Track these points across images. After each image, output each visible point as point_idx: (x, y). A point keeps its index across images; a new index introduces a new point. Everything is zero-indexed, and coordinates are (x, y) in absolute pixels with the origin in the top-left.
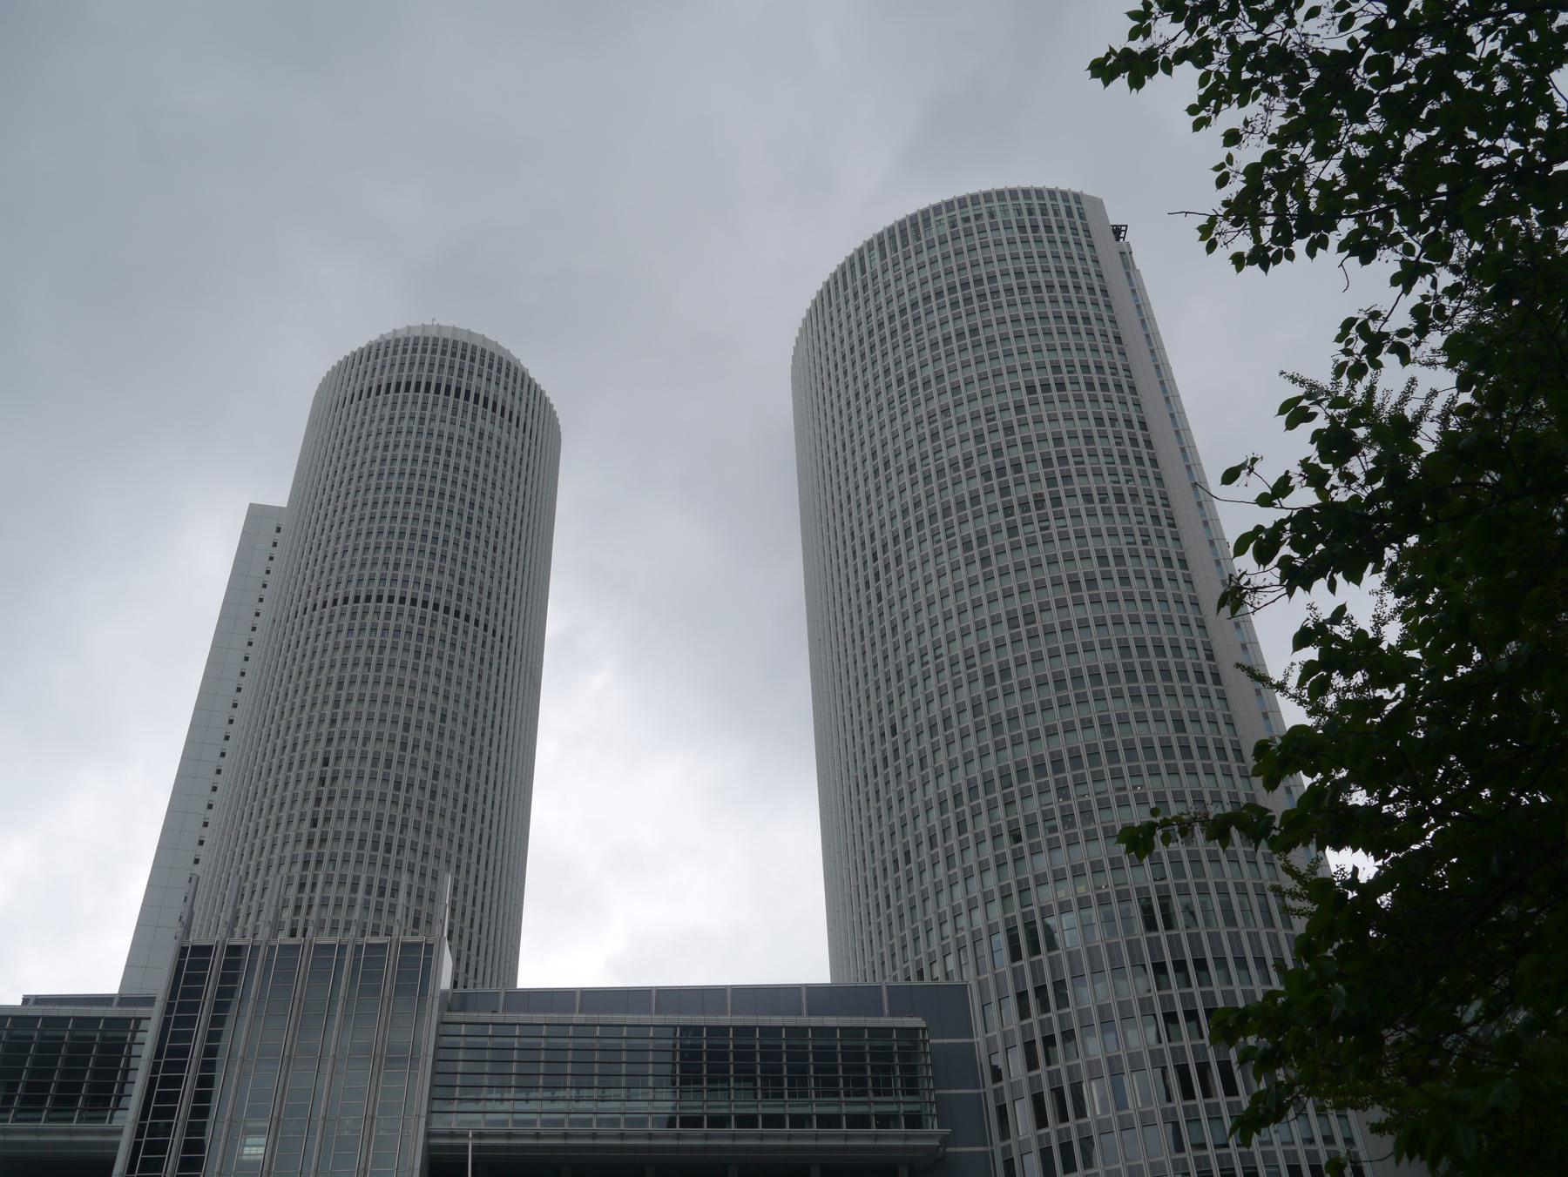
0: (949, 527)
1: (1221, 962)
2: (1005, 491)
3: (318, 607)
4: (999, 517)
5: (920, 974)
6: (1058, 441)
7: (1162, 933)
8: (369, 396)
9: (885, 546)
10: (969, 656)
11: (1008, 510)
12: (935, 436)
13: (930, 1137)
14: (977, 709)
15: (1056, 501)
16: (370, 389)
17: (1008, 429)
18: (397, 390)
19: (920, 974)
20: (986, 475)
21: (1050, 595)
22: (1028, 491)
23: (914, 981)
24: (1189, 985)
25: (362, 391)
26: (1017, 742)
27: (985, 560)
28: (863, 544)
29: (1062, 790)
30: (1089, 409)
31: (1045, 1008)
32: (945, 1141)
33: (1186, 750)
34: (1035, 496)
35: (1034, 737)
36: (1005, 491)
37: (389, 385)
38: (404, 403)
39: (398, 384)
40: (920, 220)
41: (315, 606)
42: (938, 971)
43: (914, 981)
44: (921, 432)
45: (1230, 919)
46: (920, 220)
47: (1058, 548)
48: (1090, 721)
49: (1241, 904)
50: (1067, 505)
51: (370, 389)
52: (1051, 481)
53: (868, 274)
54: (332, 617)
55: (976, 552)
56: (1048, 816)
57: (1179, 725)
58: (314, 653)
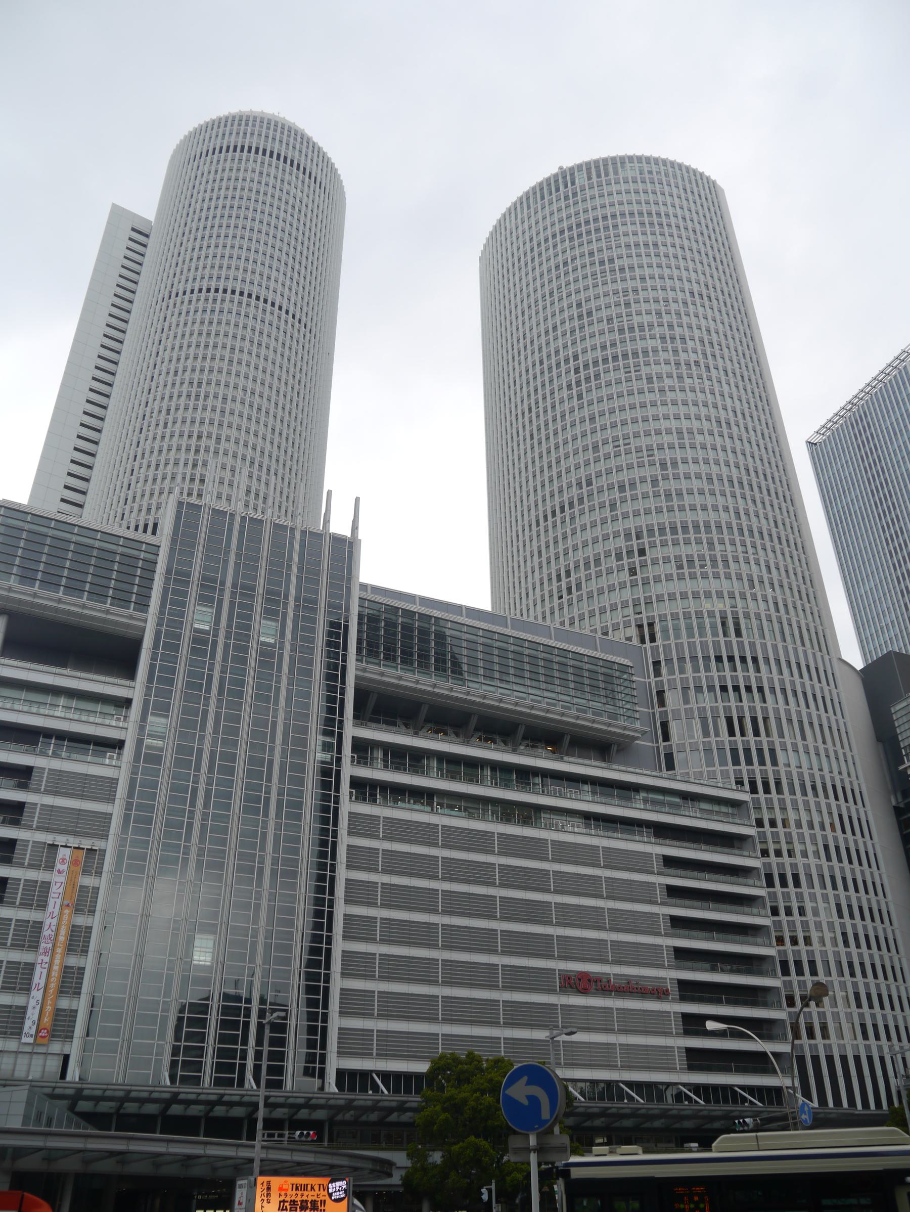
2: (675, 351)
11: (678, 364)
12: (628, 305)
13: (636, 731)
14: (655, 482)
29: (711, 544)
52: (705, 355)
56: (702, 558)
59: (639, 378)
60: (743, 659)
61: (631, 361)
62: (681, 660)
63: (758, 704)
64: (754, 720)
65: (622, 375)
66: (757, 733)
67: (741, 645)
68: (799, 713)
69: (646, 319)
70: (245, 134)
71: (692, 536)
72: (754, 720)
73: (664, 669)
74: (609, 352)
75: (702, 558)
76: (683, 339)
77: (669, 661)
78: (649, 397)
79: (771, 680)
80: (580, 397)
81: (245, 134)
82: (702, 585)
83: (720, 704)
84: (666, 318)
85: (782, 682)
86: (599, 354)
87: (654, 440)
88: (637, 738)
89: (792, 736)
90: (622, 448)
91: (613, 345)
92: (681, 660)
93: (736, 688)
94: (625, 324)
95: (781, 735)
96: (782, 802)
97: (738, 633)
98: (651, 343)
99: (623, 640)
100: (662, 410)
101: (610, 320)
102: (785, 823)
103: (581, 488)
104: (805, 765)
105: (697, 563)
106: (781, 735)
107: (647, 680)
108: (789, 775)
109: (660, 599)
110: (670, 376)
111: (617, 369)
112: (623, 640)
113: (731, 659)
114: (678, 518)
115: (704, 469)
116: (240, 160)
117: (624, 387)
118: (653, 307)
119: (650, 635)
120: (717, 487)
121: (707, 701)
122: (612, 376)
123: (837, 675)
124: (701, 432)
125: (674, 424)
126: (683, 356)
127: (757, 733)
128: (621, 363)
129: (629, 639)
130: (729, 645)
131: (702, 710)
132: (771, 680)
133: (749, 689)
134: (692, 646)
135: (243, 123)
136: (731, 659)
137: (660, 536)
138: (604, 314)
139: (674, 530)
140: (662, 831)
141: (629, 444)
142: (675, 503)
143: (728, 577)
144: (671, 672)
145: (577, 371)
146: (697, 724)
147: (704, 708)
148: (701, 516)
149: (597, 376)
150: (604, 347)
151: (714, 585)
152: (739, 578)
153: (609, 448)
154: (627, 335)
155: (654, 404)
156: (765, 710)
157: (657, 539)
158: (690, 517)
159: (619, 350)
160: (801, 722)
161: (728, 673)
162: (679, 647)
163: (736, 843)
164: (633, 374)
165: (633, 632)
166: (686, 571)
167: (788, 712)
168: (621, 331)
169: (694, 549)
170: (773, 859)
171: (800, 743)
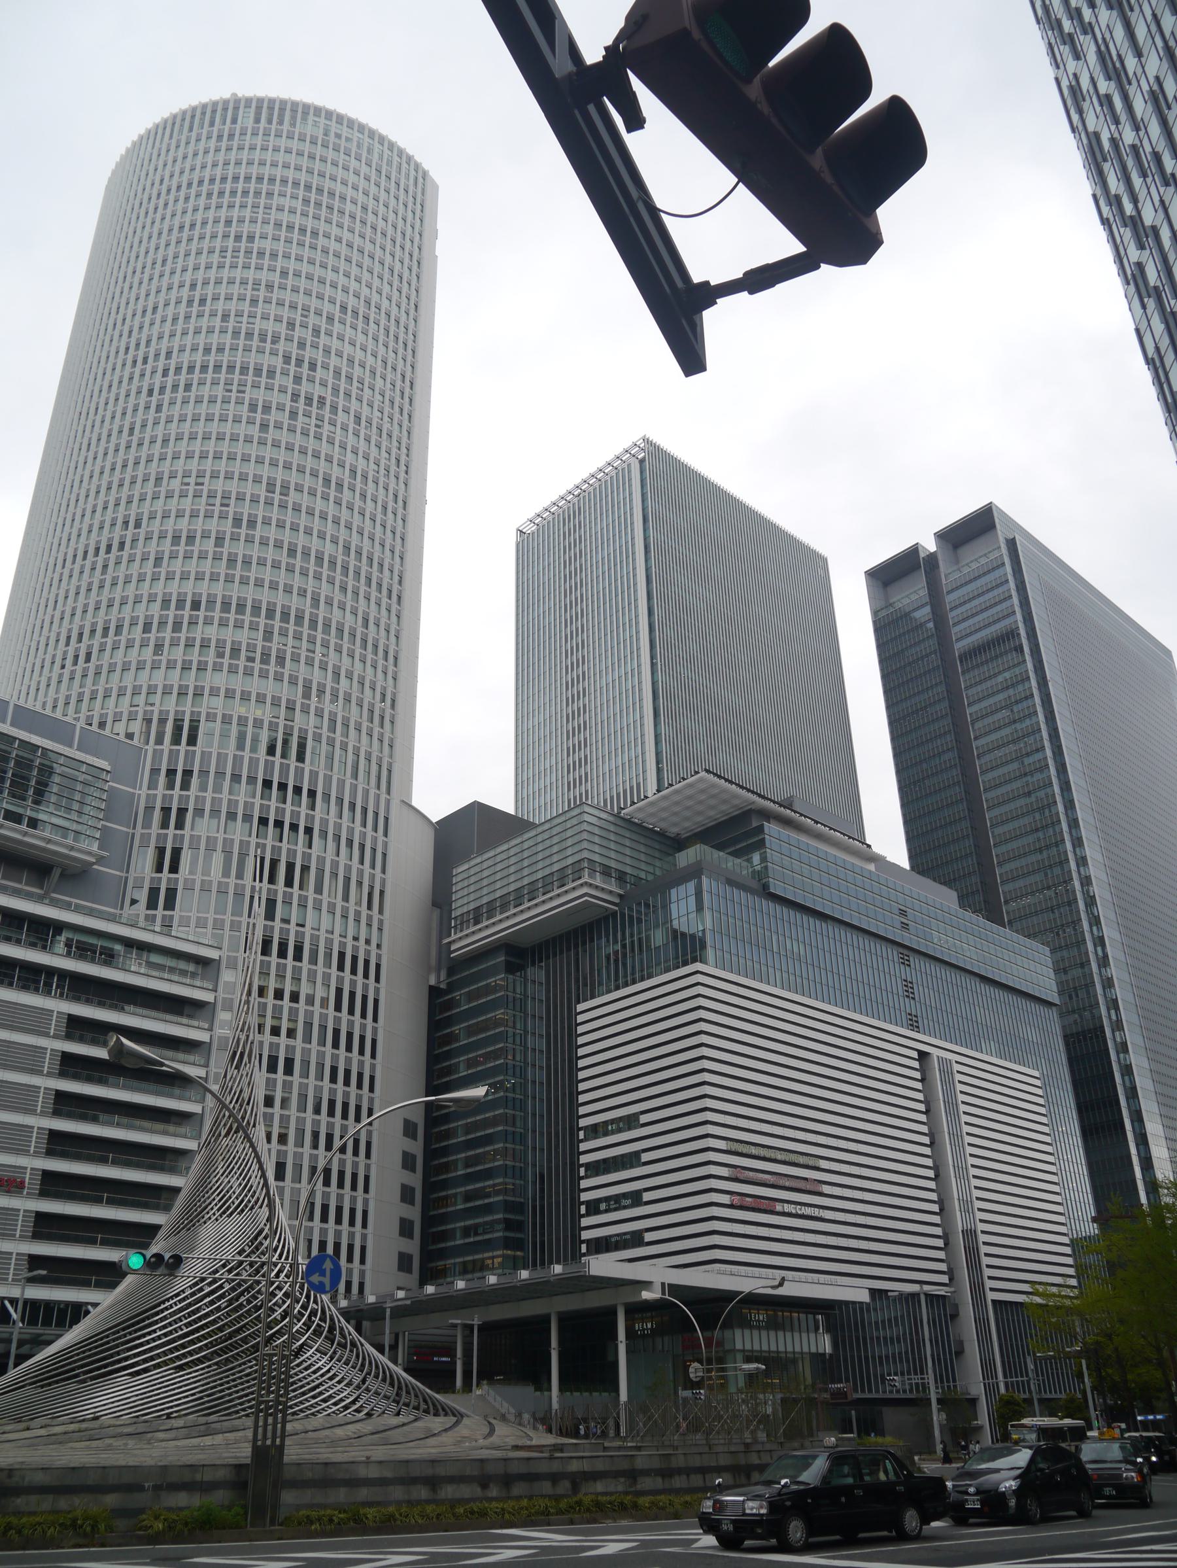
0: (242, 384)
1: (326, 797)
2: (298, 379)
4: (287, 400)
5: (102, 725)
6: (351, 361)
7: (277, 759)
9: (157, 355)
10: (226, 496)
11: (295, 397)
12: (254, 302)
13: (90, 853)
14: (219, 541)
15: (334, 409)
17: (316, 332)
19: (102, 725)
20: (287, 359)
21: (308, 481)
22: (317, 391)
23: (95, 728)
24: (284, 802)
26: (244, 581)
27: (264, 427)
28: (138, 345)
29: (268, 636)
30: (381, 350)
31: (203, 788)
32: (100, 860)
33: (313, 624)
34: (320, 397)
35: (259, 583)
36: (298, 379)
40: (300, 110)
42: (121, 728)
43: (48, 712)
44: (242, 291)
45: (355, 776)
46: (300, 110)
47: (324, 448)
48: (305, 591)
49: (314, 748)
50: (341, 417)
52: (336, 391)
53: (238, 127)
55: (259, 416)
56: (251, 648)
57: (316, 601)
59: (239, 402)
60: (298, 790)
61: (236, 377)
62: (220, 774)
63: (300, 848)
64: (290, 867)
65: (219, 391)
66: (289, 883)
67: (299, 773)
68: (348, 868)
69: (270, 326)
71: (247, 618)
72: (290, 867)
73: (195, 781)
74: (212, 359)
75: (251, 648)
76: (313, 366)
77: (204, 773)
78: (242, 429)
79: (324, 822)
80: (159, 408)
82: (255, 685)
83: (253, 840)
84: (298, 332)
85: (338, 826)
86: (199, 357)
87: (233, 487)
88: (94, 863)
89: (333, 895)
90: (191, 488)
91: (220, 350)
92: (220, 774)
93: (279, 824)
94: (244, 326)
95: (319, 890)
96: (297, 972)
97: (301, 758)
98: (266, 361)
99: (122, 737)
100: (253, 450)
101: (225, 317)
102: (295, 997)
103: (127, 529)
104: (337, 930)
105: (243, 654)
106: (319, 890)
107: (137, 792)
108: (315, 940)
109: (214, 692)
110: (281, 408)
111: (215, 383)
112: (122, 737)
113: (283, 787)
114: (235, 592)
115: (287, 536)
117: (217, 410)
118: (286, 313)
119: (189, 735)
120: (298, 562)
121: (238, 832)
122: (206, 391)
123: (392, 821)
124: (300, 489)
125: (265, 471)
126: (304, 387)
127: (289, 883)
128: (223, 376)
129: (130, 736)
130: (285, 769)
131: (228, 843)
132: (324, 822)
133: (294, 827)
134: (238, 760)
136: (283, 787)
137: (236, 613)
138: (220, 306)
139: (256, 610)
140: (80, 987)
141: (202, 484)
142: (238, 572)
143: (279, 678)
144: (203, 788)
145: (165, 373)
146: (218, 859)
147: (232, 840)
148: (265, 596)
149: (188, 387)
150: (207, 351)
151: (255, 685)
152: (293, 681)
153: (176, 484)
154: (241, 342)
155: (248, 440)
156: (307, 857)
157: (232, 616)
158: (250, 593)
159: (225, 359)
160: (347, 880)
161: (273, 804)
162: (221, 758)
163: (187, 1010)
164: (234, 395)
165: (136, 727)
166: (257, 665)
167: (335, 864)
168: (236, 334)
169: (243, 636)
170: (283, 1040)
171: (339, 903)
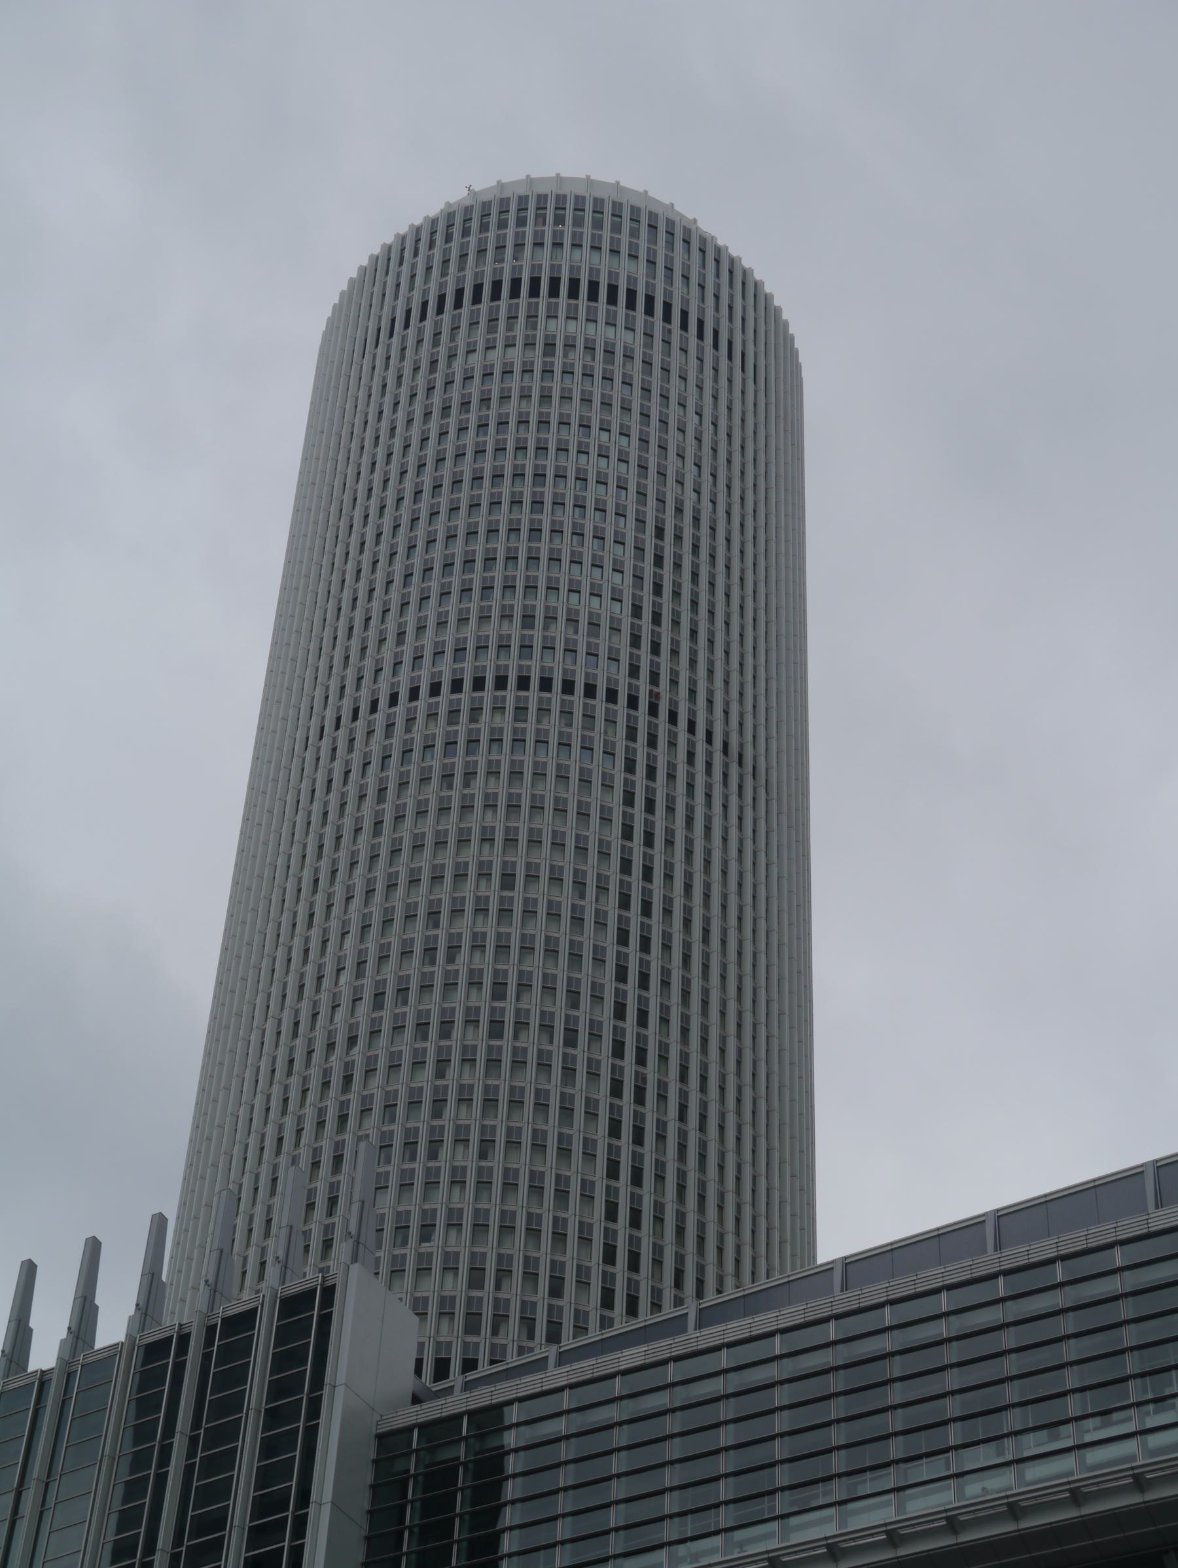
3: (361, 713)
8: (423, 317)
16: (425, 305)
18: (477, 299)
25: (408, 312)
37: (459, 293)
38: (512, 318)
39: (478, 289)
41: (356, 711)
51: (425, 305)
54: (390, 726)
58: (382, 791)
70: (500, 248)
81: (500, 248)
116: (493, 320)
135: (512, 217)
